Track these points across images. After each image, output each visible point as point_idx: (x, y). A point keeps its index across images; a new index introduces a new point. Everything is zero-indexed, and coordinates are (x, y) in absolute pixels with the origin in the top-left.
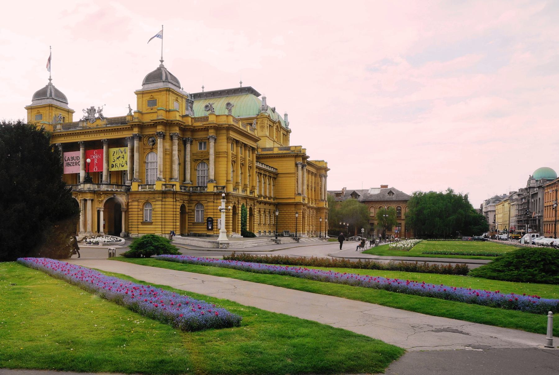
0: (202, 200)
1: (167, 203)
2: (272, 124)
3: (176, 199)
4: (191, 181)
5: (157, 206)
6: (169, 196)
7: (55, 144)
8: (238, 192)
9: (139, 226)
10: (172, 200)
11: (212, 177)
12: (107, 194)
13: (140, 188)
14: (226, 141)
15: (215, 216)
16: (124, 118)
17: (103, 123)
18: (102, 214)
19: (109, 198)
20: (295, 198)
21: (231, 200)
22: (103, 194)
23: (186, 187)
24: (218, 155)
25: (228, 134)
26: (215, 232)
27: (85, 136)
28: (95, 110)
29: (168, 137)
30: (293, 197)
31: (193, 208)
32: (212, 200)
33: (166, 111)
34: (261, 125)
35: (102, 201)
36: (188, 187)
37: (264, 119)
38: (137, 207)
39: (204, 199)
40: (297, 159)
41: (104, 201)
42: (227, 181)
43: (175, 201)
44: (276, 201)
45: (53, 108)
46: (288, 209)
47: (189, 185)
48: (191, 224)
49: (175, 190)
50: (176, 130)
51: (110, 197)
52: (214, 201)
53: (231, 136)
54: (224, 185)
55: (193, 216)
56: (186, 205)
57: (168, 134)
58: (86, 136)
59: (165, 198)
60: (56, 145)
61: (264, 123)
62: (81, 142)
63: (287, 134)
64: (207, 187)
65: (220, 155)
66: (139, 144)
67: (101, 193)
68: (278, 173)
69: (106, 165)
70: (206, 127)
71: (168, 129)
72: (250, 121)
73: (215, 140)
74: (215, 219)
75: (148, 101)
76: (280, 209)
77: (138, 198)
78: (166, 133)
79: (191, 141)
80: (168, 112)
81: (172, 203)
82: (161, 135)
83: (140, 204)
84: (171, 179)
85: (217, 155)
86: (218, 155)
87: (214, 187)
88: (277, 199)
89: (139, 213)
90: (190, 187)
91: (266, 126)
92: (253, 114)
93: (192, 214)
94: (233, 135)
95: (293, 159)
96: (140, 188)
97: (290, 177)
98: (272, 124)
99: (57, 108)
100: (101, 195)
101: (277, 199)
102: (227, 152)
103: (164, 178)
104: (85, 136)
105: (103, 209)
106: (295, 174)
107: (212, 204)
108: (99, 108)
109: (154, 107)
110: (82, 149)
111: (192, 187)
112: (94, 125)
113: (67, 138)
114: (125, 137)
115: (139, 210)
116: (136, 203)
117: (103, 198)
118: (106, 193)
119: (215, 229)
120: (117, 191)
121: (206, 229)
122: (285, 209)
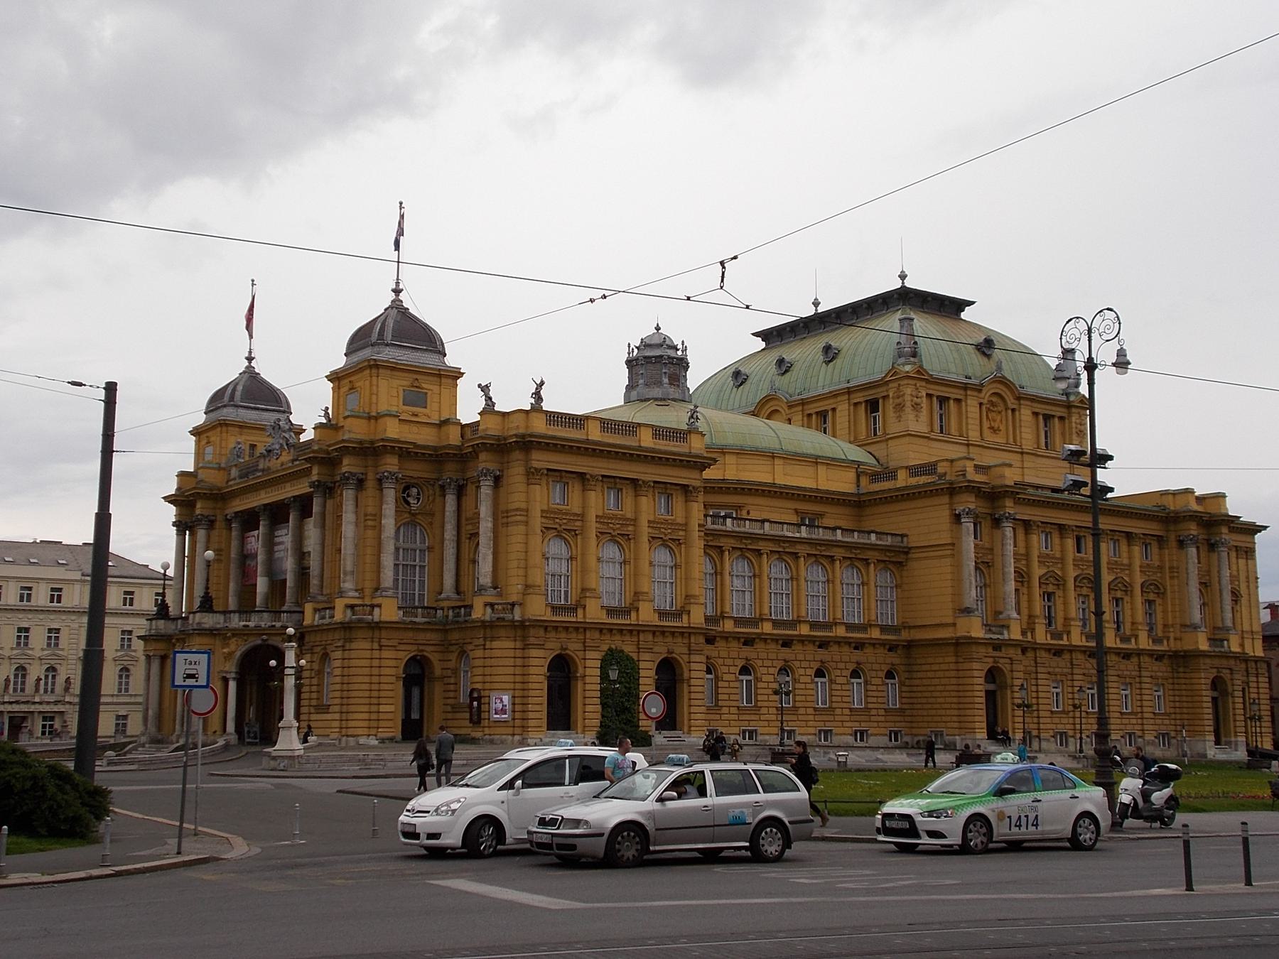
0: (466, 641)
1: (354, 654)
2: (954, 393)
3: (380, 642)
4: (458, 593)
6: (360, 634)
7: (227, 515)
8: (584, 617)
10: (367, 645)
11: (485, 577)
12: (244, 635)
14: (521, 479)
15: (487, 686)
18: (232, 685)
19: (247, 647)
20: (954, 625)
21: (532, 640)
22: (234, 635)
23: (436, 609)
24: (505, 520)
25: (527, 461)
26: (487, 731)
29: (371, 483)
30: (950, 620)
31: (452, 664)
32: (481, 641)
33: (369, 418)
34: (898, 401)
35: (231, 654)
36: (442, 609)
37: (902, 383)
40: (957, 498)
41: (238, 654)
42: (527, 586)
43: (376, 646)
44: (905, 635)
45: (230, 428)
46: (930, 660)
47: (445, 604)
48: (449, 709)
49: (376, 618)
50: (386, 464)
51: (252, 644)
52: (484, 645)
53: (535, 464)
54: (514, 598)
55: (452, 687)
56: (434, 658)
57: (371, 476)
59: (350, 640)
60: (228, 517)
61: (904, 395)
63: (1070, 414)
64: (471, 607)
65: (509, 519)
67: (229, 634)
68: (910, 548)
70: (473, 446)
71: (370, 463)
72: (871, 394)
73: (497, 480)
74: (486, 693)
76: (919, 661)
78: (366, 474)
79: (459, 486)
80: (372, 421)
81: (368, 654)
82: (348, 479)
84: (377, 589)
85: (501, 517)
86: (505, 520)
87: (486, 605)
88: (910, 628)
90: (449, 608)
91: (908, 404)
92: (876, 371)
93: (452, 681)
94: (541, 460)
95: (946, 499)
97: (926, 558)
98: (962, 392)
99: (242, 427)
100: (229, 638)
101: (910, 628)
102: (527, 510)
103: (356, 590)
105: (233, 675)
106: (954, 546)
107: (479, 653)
110: (264, 526)
111: (453, 608)
117: (233, 647)
118: (237, 633)
119: (486, 723)
120: (274, 626)
122: (930, 660)
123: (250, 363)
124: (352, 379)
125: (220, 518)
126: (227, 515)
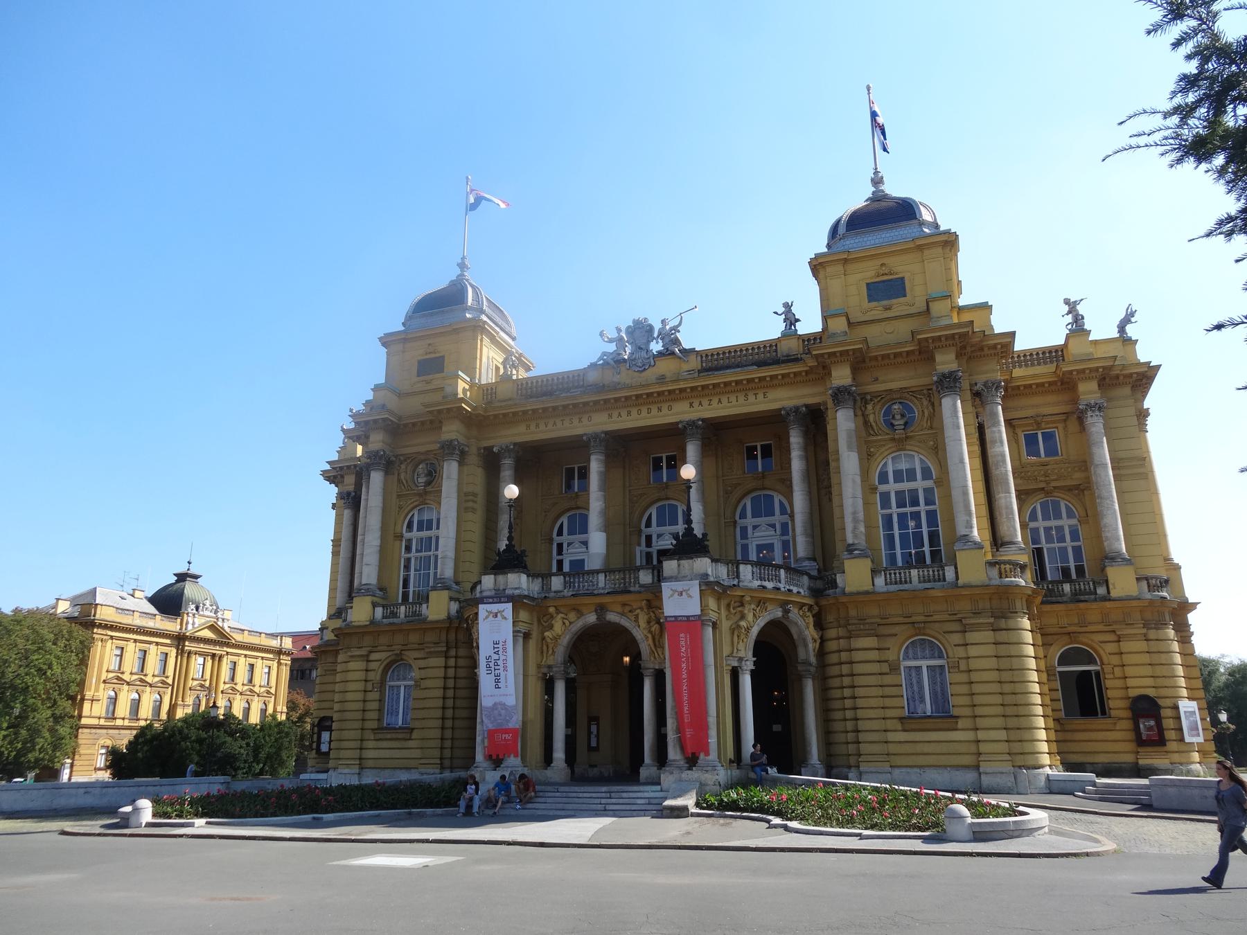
5: (973, 651)
7: (493, 447)
9: (891, 736)
13: (880, 581)
16: (771, 345)
17: (685, 367)
18: (746, 682)
27: (610, 416)
28: (650, 329)
38: (874, 655)
39: (1101, 627)
41: (755, 631)
58: (615, 414)
62: (595, 436)
66: (855, 423)
69: (701, 508)
75: (868, 284)
77: (879, 620)
83: (889, 643)
89: (888, 680)
96: (880, 581)
104: (610, 416)
105: (749, 665)
108: (663, 322)
109: (894, 301)
112: (651, 374)
113: (537, 426)
114: (780, 410)
115: (885, 668)
116: (870, 642)
121: (1131, 746)
123: (462, 270)
124: (885, 261)
125: (474, 450)
126: (493, 447)
